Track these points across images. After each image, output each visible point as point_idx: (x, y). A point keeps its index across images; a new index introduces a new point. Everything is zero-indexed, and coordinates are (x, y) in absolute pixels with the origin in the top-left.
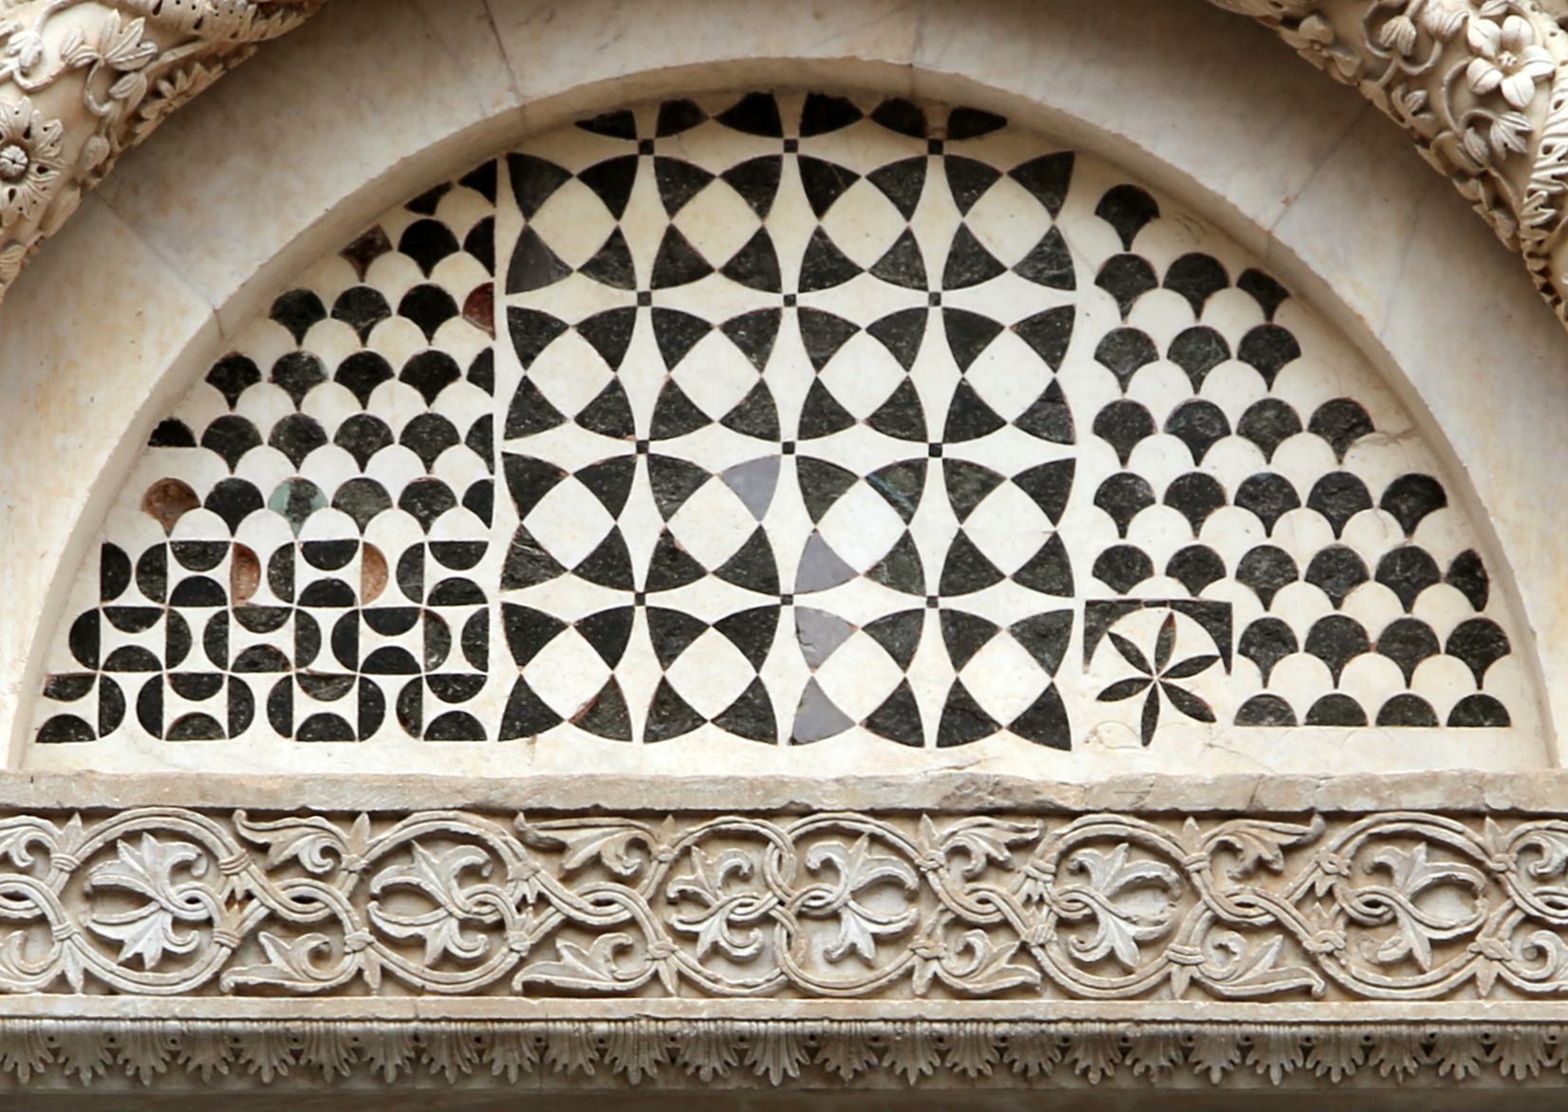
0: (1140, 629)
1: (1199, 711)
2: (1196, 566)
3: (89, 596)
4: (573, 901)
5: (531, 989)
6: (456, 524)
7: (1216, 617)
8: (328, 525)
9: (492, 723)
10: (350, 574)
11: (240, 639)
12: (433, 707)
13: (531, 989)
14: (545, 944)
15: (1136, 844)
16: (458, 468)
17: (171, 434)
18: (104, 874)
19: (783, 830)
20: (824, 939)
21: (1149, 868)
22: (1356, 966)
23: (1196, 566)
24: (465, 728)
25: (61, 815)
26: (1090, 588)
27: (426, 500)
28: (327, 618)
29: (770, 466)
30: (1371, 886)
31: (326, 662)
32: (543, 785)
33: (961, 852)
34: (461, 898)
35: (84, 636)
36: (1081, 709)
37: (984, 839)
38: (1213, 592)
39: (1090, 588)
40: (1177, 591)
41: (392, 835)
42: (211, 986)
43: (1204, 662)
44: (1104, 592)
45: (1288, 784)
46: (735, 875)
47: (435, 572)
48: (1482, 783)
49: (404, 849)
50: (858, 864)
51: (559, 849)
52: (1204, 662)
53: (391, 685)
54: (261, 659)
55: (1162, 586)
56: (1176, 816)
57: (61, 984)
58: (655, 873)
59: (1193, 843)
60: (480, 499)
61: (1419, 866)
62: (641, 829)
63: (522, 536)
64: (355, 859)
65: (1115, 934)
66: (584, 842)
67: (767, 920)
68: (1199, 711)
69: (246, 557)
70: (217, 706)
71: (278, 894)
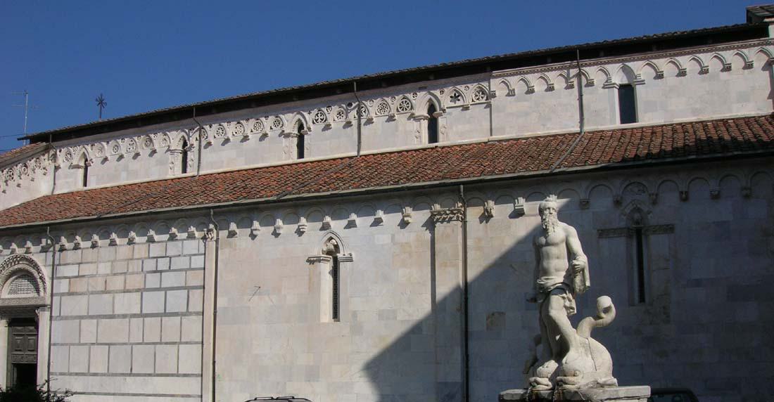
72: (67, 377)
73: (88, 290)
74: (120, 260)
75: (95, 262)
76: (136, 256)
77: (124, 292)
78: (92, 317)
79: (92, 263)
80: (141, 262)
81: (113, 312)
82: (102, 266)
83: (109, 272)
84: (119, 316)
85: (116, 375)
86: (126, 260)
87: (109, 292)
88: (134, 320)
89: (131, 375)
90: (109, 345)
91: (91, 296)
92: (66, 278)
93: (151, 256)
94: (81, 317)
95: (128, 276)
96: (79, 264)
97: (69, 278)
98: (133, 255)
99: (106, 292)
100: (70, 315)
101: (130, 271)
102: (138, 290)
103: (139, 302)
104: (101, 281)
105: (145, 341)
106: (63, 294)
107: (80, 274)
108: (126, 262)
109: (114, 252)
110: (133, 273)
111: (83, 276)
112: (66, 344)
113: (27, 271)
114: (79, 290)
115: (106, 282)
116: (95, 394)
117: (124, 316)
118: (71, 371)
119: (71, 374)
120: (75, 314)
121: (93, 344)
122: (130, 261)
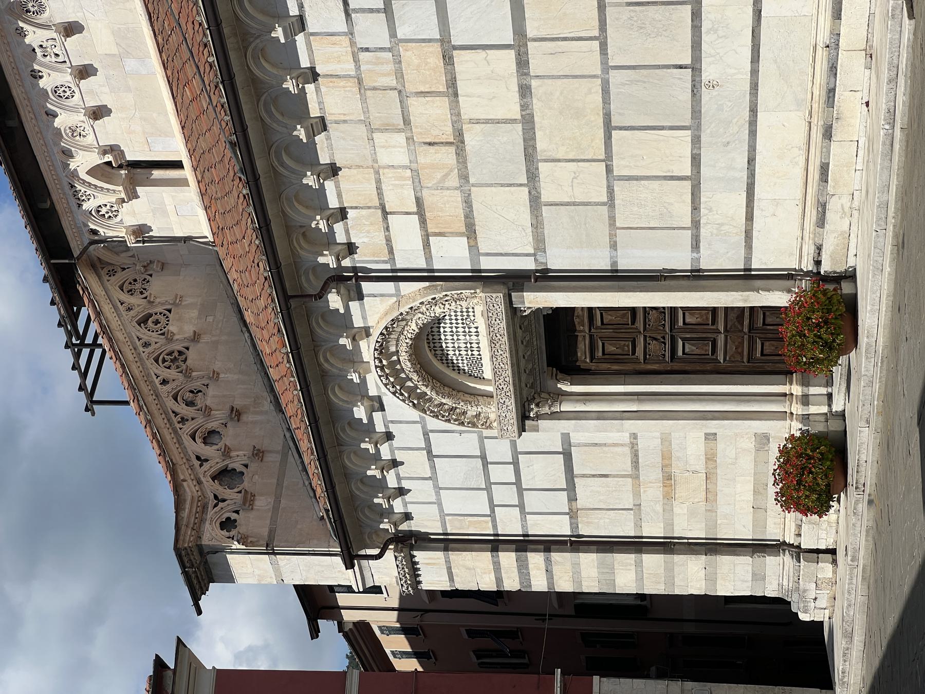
0: (468, 323)
6: (464, 358)
7: (466, 319)
8: (465, 365)
16: (460, 358)
17: (459, 373)
23: (462, 319)
24: (481, 358)
26: (465, 325)
36: (475, 326)
39: (465, 325)
66: (497, 379)
71: (504, 394)
72: (703, 231)
73: (456, 189)
74: (366, 111)
75: (377, 173)
76: (349, 67)
77: (456, 95)
78: (533, 176)
79: (378, 182)
80: (363, 56)
81: (514, 121)
82: (384, 158)
83: (401, 138)
84: (524, 107)
85: (696, 113)
86: (364, 100)
87: (459, 135)
88: (535, 66)
89: (695, 68)
90: (609, 128)
91: (472, 180)
92: (427, 245)
93: (343, 28)
94: (535, 202)
95: (410, 88)
96: (385, 214)
98: (350, 76)
99: (459, 142)
101: (394, 83)
102: (448, 60)
103: (481, 54)
104: (428, 157)
105: (596, 33)
106: (473, 248)
107: (415, 210)
108: (369, 93)
109: (342, 127)
110: (399, 75)
111: (419, 202)
112: (612, 236)
114: (461, 213)
115: (430, 144)
116: (751, 161)
117: (525, 91)
118: (687, 222)
119: (696, 224)
120: (526, 218)
121: (609, 170)
122: (367, 83)
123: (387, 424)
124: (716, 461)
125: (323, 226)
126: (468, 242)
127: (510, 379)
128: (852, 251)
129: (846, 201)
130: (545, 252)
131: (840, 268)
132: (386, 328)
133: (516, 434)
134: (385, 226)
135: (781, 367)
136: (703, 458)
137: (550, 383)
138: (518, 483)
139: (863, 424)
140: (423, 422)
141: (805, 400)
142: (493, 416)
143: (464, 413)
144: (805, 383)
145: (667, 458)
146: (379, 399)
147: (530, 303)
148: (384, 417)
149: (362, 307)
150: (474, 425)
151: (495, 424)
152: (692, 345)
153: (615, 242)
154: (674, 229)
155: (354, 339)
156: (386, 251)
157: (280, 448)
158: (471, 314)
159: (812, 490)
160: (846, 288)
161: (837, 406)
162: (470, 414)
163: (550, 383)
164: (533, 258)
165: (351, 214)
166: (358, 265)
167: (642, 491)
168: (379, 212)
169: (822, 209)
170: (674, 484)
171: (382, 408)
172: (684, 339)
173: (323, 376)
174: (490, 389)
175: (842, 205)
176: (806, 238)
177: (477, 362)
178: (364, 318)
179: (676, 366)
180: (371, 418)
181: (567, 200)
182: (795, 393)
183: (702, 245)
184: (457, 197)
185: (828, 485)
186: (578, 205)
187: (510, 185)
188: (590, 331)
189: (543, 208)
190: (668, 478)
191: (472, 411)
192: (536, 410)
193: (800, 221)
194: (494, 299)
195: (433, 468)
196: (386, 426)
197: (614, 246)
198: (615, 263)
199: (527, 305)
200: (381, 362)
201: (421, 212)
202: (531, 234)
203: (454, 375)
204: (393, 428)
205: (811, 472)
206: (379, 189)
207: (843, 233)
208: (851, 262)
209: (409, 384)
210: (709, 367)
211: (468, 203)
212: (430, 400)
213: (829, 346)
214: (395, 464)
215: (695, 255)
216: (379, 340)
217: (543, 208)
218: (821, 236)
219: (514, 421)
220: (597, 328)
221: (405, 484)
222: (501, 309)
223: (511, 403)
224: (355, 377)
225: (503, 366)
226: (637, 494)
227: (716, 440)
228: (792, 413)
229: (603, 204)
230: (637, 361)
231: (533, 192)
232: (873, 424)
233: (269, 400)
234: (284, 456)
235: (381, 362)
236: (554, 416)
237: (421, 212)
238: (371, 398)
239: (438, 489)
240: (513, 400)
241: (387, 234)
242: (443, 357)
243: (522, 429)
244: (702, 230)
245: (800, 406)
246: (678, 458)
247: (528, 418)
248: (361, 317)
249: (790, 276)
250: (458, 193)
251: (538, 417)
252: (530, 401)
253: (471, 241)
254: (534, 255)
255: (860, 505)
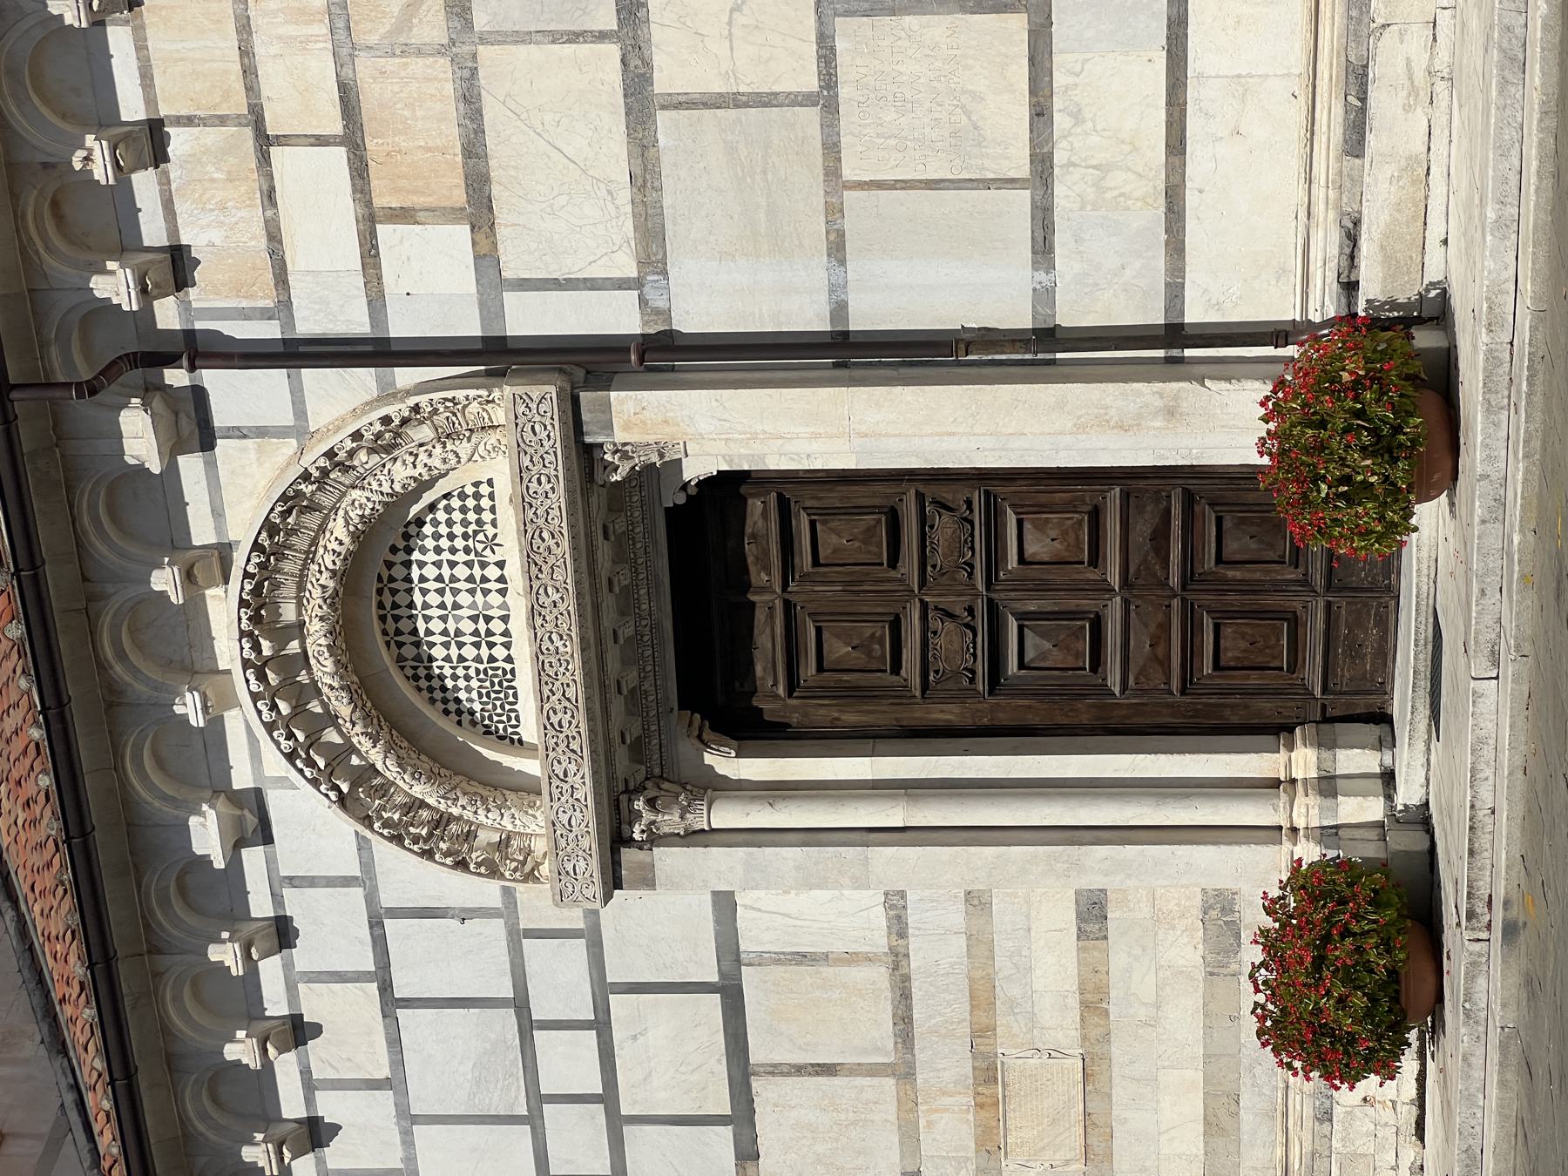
0: (480, 547)
1: (495, 535)
2: (465, 536)
3: (494, 737)
4: (559, 695)
5: (577, 702)
6: (472, 672)
7: (476, 533)
8: (474, 695)
9: (512, 666)
10: (484, 691)
11: (499, 711)
12: (509, 676)
13: (577, 702)
14: (568, 699)
15: (537, 593)
16: (460, 672)
18: (562, 777)
19: (541, 657)
20: (561, 649)
21: (542, 591)
22: (559, 551)
23: (465, 536)
24: (513, 671)
25: (550, 783)
26: (472, 556)
27: (467, 678)
28: (493, 695)
29: (454, 616)
30: (541, 550)
31: (502, 695)
32: (536, 700)
33: (542, 625)
34: (560, 715)
35: (502, 738)
36: (497, 558)
37: (539, 621)
38: (471, 533)
39: (472, 556)
40: (471, 540)
41: (549, 727)
42: (582, 757)
43: (485, 535)
44: (473, 553)
45: (522, 566)
46: (551, 666)
47: (482, 676)
48: (518, 530)
49: (552, 724)
50: (546, 644)
51: (548, 697)
52: (485, 535)
53: (505, 684)
54: (502, 707)
55: (470, 542)
56: (531, 587)
57: (584, 783)
58: (551, 680)
59: (536, 584)
60: (466, 668)
61: (537, 540)
62: (543, 683)
63: (473, 660)
64: (554, 733)
65: (556, 597)
66: (546, 692)
67: (559, 660)
68: (495, 535)
69: (482, 710)
70: (513, 715)
71: (563, 746)
73: (441, 51)
91: (481, 21)
96: (265, 142)
97: (369, 221)
100: (625, 194)
107: (336, 127)
112: (834, 212)
113: (349, 576)
114: (451, 136)
118: (1020, 166)
123: (277, 890)
124: (1107, 1013)
125: (101, 171)
126: (474, 243)
127: (576, 691)
128: (1435, 232)
129: (1418, 37)
130: (665, 273)
131: (1406, 292)
132: (269, 527)
133: (597, 889)
134: (265, 188)
135: (1266, 707)
136: (1074, 1002)
137: (686, 746)
138: (608, 1097)
139: (1481, 666)
140: (366, 879)
141: (1328, 785)
142: (540, 846)
143: (469, 836)
144: (1326, 744)
145: (982, 997)
146: (255, 800)
147: (626, 427)
148: (271, 863)
149: (211, 466)
150: (493, 872)
151: (545, 869)
152: (1043, 635)
153: (841, 235)
154: (986, 184)
155: (189, 576)
156: (269, 276)
157: (45, 1129)
158: (487, 516)
159: (1350, 979)
160: (1424, 339)
161: (1408, 794)
162: (484, 837)
163: (686, 746)
164: (636, 293)
165: (179, 141)
166: (199, 325)
167: (922, 1123)
168: (248, 133)
169: (1358, 79)
170: (1004, 1097)
171: (265, 836)
172: (1022, 617)
173: (110, 705)
174: (532, 767)
175: (1408, 61)
176: (1319, 208)
177: (502, 683)
178: (218, 513)
179: (1007, 709)
180: (235, 864)
181: (718, 87)
182: (1298, 774)
183: (1060, 240)
184: (440, 78)
185: (1393, 973)
186: (746, 105)
187: (575, 37)
188: (785, 586)
189: (661, 116)
190: (988, 1073)
191: (491, 822)
192: (647, 816)
193: (1297, 149)
194: (533, 406)
195: (395, 1042)
196: (277, 899)
197: (837, 249)
198: (840, 309)
199: (620, 436)
200: (256, 647)
201: (353, 139)
202: (629, 208)
203: (447, 725)
204: (296, 905)
205: (1346, 933)
206: (246, 52)
207: (1412, 159)
208: (1434, 274)
209: (332, 736)
210: (1084, 712)
211: (470, 100)
212: (384, 790)
213: (1384, 447)
214: (298, 1031)
215: (1041, 276)
216: (251, 569)
217: (661, 116)
218: (1357, 181)
219: (590, 842)
220: (805, 577)
221: (329, 1107)
222: (551, 436)
223: (582, 782)
224: (189, 707)
225: (559, 644)
226: (910, 1136)
227: (1105, 938)
228: (1294, 830)
229: (807, 100)
230: (900, 695)
231: (634, 62)
232: (1508, 670)
233: (39, 1038)
234: (53, 1146)
235: (256, 647)
236: (694, 837)
237: (353, 139)
238: (237, 799)
239: (408, 1119)
240: (586, 769)
241: (269, 213)
242: (419, 669)
243: (613, 881)
244: (1059, 189)
245: (1314, 800)
246: (1012, 1004)
247: (629, 842)
248: (209, 510)
249: (1278, 334)
250: (443, 63)
251: (654, 839)
252: (632, 792)
253: (480, 237)
254: (637, 284)
255: (1481, 982)
